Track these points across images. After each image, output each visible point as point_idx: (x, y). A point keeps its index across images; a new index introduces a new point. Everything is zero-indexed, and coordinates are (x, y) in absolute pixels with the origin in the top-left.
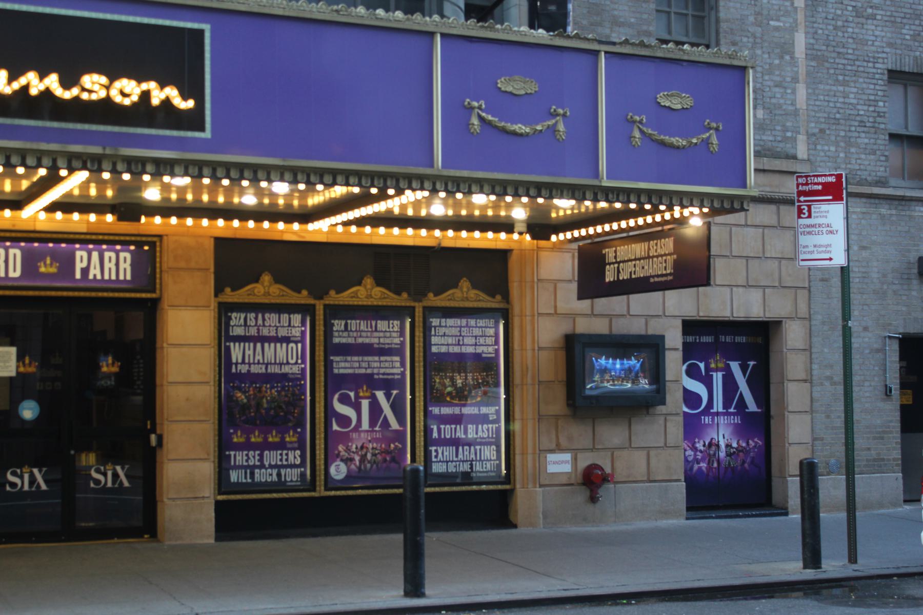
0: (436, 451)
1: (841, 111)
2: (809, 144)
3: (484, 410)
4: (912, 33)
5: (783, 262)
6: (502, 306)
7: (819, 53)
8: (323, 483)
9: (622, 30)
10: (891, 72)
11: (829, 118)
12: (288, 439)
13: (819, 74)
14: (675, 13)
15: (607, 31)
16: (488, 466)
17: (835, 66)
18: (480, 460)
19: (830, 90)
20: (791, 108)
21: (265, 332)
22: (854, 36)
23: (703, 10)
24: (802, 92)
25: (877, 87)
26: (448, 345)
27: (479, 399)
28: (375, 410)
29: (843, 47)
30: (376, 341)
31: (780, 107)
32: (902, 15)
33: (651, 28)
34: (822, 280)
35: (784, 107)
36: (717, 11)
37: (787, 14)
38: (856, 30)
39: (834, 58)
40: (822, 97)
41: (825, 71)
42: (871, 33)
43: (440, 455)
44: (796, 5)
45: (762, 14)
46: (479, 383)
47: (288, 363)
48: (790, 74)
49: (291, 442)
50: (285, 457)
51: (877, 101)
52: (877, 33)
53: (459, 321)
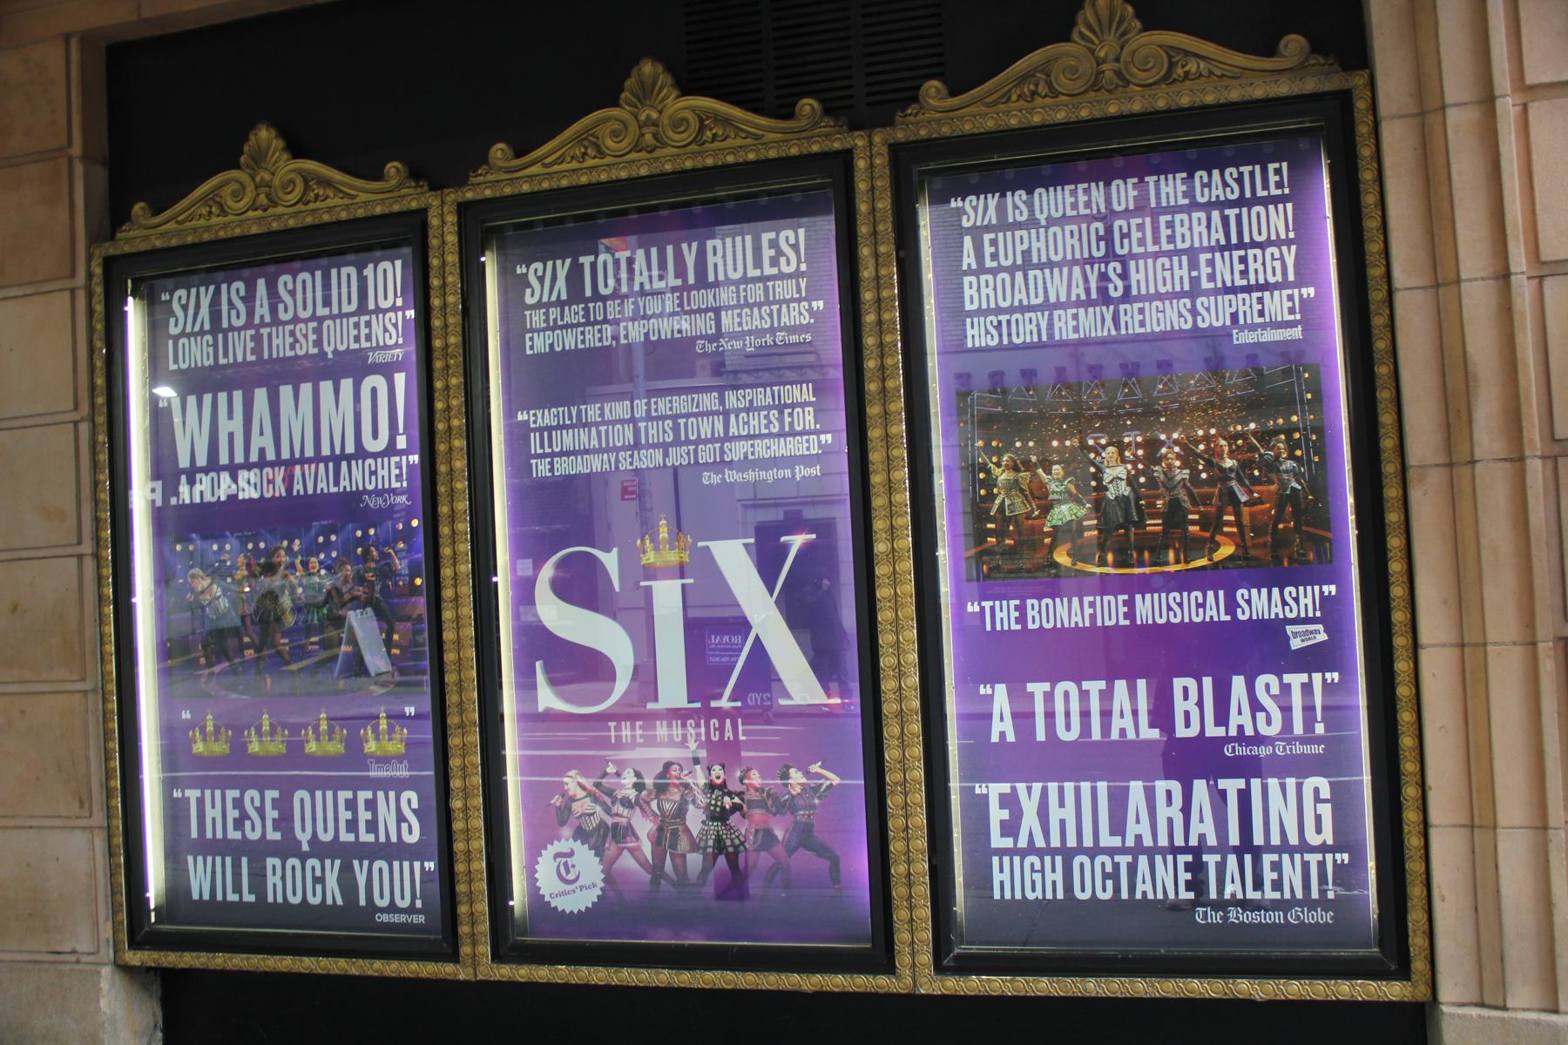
0: (1010, 801)
3: (1258, 603)
6: (1309, 85)
8: (484, 926)
12: (371, 747)
16: (1292, 875)
18: (1246, 845)
21: (280, 345)
26: (1047, 306)
27: (1226, 550)
28: (713, 628)
30: (705, 325)
43: (1030, 821)
46: (1224, 476)
47: (361, 453)
49: (384, 760)
50: (364, 816)
53: (1097, 193)
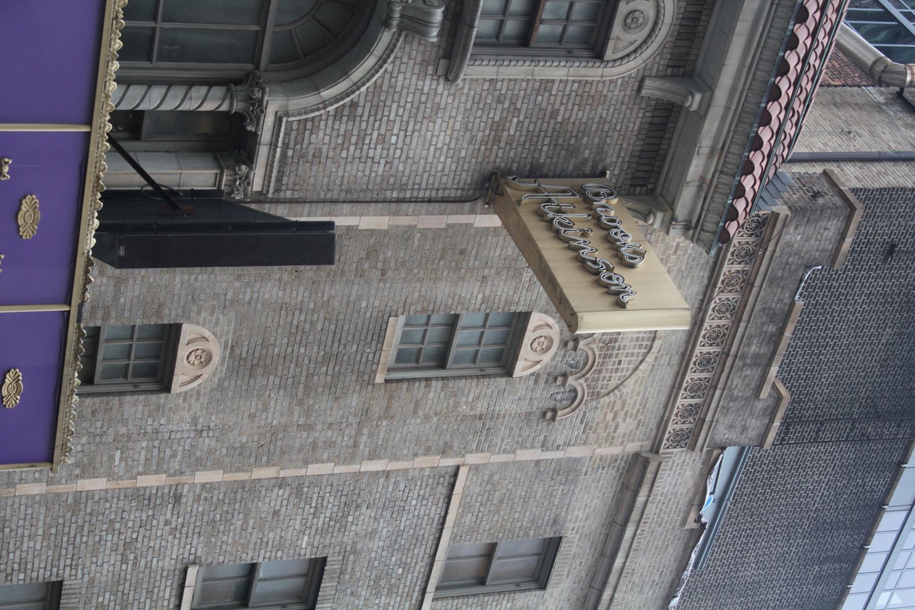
1: (13, 534)
4: (106, 603)
7: (82, 506)
9: (111, 288)
10: (60, 584)
13: (57, 507)
14: (131, 346)
19: (38, 520)
22: (102, 543)
23: (133, 377)
25: (42, 571)
29: (89, 532)
32: (126, 591)
33: (112, 321)
36: (132, 393)
37: (129, 469)
38: (109, 544)
40: (29, 512)
41: (61, 514)
42: (106, 559)
44: (139, 477)
45: (128, 441)
51: (25, 572)
52: (105, 566)
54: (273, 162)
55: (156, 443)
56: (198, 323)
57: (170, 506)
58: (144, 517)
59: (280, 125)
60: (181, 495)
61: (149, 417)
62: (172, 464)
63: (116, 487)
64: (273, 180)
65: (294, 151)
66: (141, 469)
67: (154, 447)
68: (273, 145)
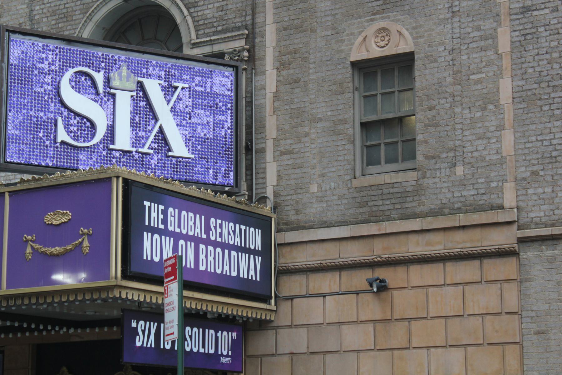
2: (517, 190)
5: (488, 317)
9: (319, 125)
11: (543, 157)
13: (530, 115)
15: (306, 129)
17: (551, 101)
19: (544, 128)
20: (495, 157)
24: (508, 138)
31: (483, 158)
33: (346, 116)
34: (538, 333)
35: (488, 158)
37: (490, 63)
39: (549, 94)
41: (539, 109)
44: (500, 52)
48: (494, 123)
54: (222, 39)
55: (463, 47)
56: (350, 50)
57: (535, 13)
58: (547, 33)
59: (200, 42)
60: (523, 7)
61: (437, 61)
62: (487, 27)
63: (509, 68)
64: (233, 34)
65: (219, 26)
66: (491, 53)
67: (468, 47)
68: (211, 43)
